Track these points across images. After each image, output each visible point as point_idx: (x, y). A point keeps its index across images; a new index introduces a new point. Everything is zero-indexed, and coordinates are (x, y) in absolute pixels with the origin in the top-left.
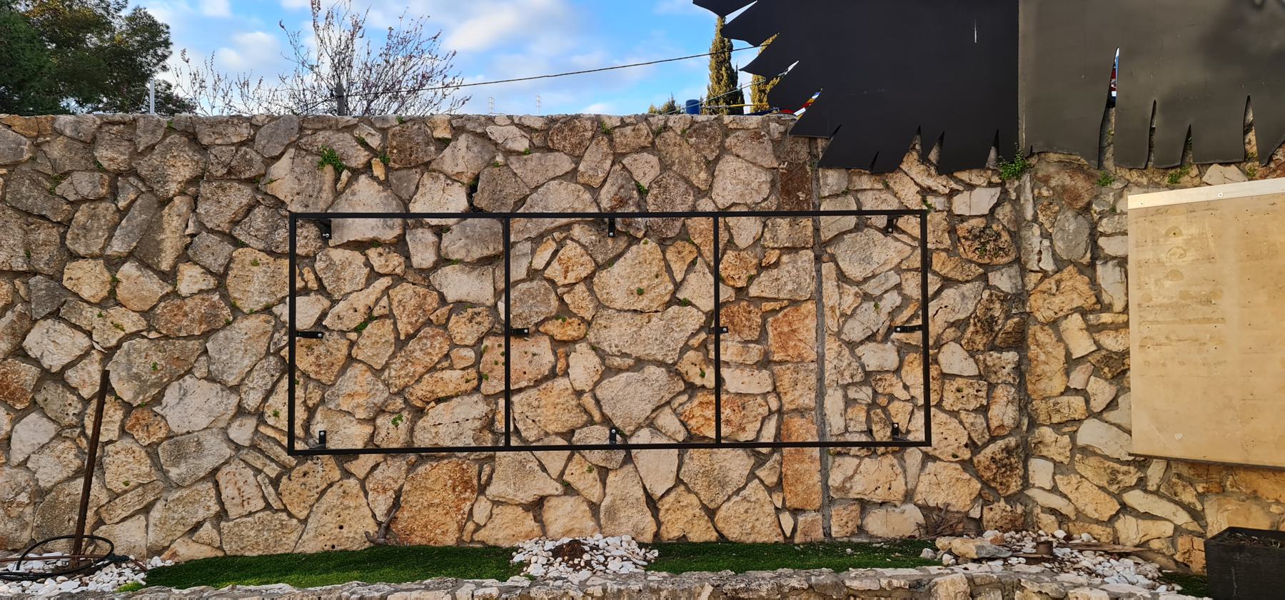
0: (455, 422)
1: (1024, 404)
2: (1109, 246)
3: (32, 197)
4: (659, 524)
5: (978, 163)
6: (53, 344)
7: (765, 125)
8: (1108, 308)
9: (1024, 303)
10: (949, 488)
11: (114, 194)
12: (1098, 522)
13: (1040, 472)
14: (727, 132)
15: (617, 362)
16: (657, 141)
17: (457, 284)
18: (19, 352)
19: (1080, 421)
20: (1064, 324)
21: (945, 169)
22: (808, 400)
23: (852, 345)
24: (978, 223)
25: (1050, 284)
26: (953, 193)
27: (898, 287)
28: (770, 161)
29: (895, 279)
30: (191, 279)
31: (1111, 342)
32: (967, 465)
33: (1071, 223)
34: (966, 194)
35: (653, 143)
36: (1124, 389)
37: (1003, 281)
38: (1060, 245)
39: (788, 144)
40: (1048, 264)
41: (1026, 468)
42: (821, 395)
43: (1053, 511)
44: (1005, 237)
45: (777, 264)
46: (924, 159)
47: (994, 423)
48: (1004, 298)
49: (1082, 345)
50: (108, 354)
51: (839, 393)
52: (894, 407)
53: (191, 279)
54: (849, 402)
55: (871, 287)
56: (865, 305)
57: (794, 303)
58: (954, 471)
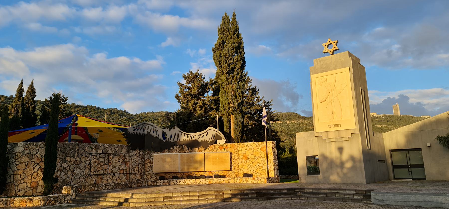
0: (100, 172)
1: (144, 170)
2: (152, 157)
3: (64, 151)
6: (65, 165)
10: (138, 177)
11: (71, 151)
17: (101, 160)
18: (61, 166)
21: (139, 150)
30: (78, 159)
31: (152, 165)
37: (143, 160)
49: (149, 165)
50: (70, 166)
53: (78, 159)
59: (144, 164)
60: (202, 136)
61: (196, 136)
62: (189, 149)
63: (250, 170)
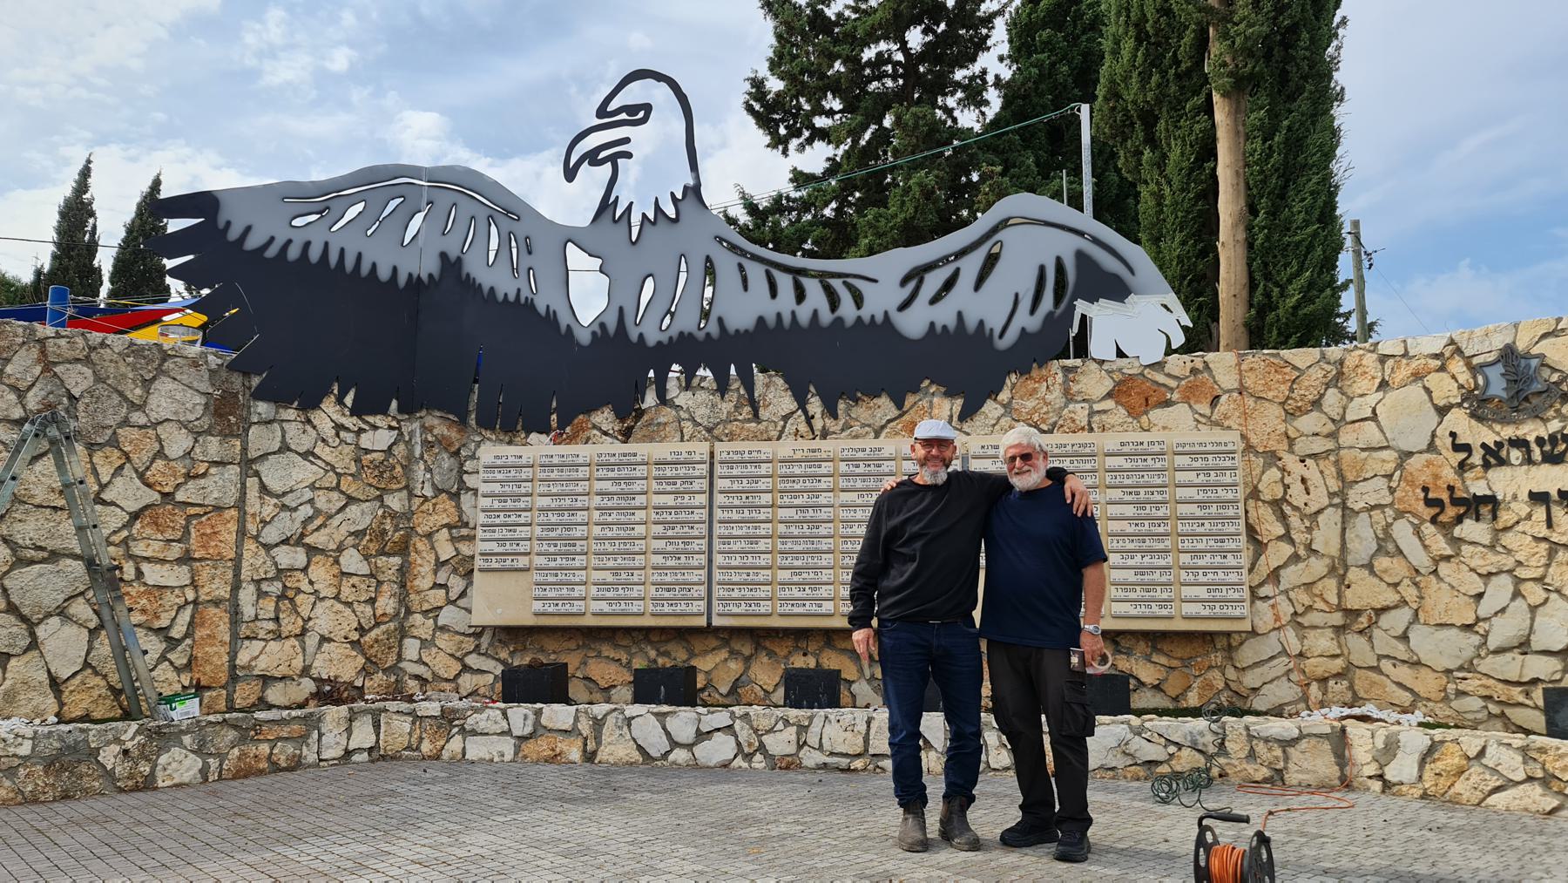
1: (403, 600)
2: (470, 481)
4: (62, 704)
5: (384, 411)
7: (204, 355)
8: (466, 525)
9: (409, 520)
10: (340, 664)
12: (447, 680)
13: (411, 648)
14: (165, 356)
15: (31, 553)
16: (93, 355)
19: (441, 608)
20: (436, 537)
21: (356, 411)
22: (224, 592)
23: (268, 547)
24: (379, 457)
25: (428, 506)
26: (361, 431)
27: (311, 501)
28: (205, 386)
29: (308, 495)
31: (465, 549)
32: (355, 644)
33: (447, 462)
34: (371, 433)
35: (88, 357)
36: (470, 583)
37: (395, 502)
38: (437, 478)
39: (224, 374)
40: (428, 492)
41: (400, 646)
42: (236, 587)
43: (417, 677)
44: (399, 469)
45: (204, 475)
46: (340, 401)
47: (379, 612)
48: (394, 516)
49: (446, 552)
51: (252, 588)
52: (299, 599)
54: (261, 594)
55: (287, 500)
56: (282, 514)
57: (218, 509)
58: (346, 649)
59: (393, 541)
60: (934, 281)
61: (881, 280)
62: (815, 406)
63: (1503, 631)
